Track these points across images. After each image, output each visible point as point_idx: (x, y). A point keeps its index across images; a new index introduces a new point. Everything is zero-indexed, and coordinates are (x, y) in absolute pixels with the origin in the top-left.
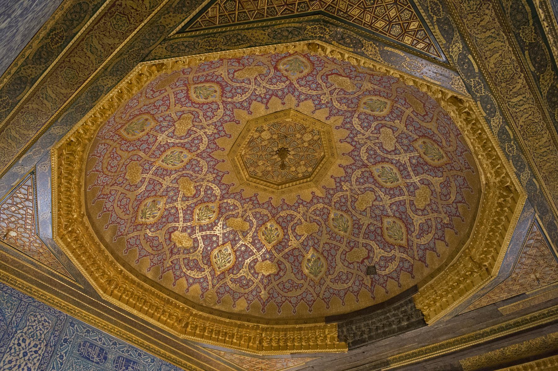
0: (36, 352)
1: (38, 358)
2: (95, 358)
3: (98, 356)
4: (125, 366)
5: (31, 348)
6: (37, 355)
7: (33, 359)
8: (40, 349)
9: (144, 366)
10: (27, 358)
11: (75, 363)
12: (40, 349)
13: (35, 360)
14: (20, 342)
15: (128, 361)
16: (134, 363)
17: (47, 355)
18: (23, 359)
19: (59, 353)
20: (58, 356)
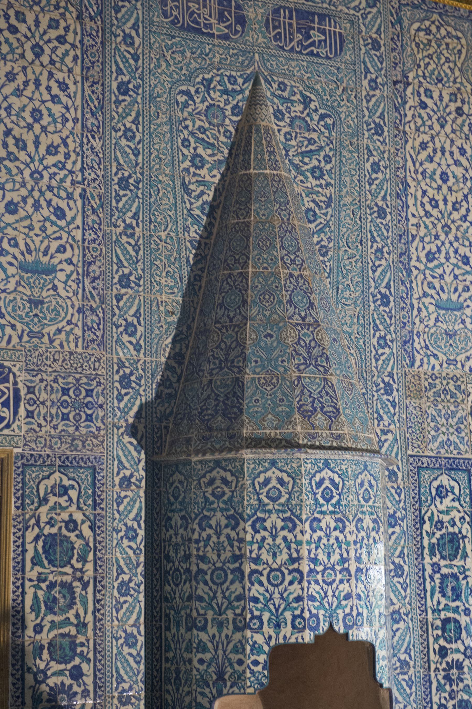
0: (61, 40)
1: (72, 53)
2: (215, 26)
3: (221, 18)
4: (299, 31)
5: (45, 33)
6: (68, 46)
7: (62, 60)
8: (67, 29)
9: (352, 22)
10: (45, 59)
11: (168, 48)
12: (67, 29)
13: (69, 60)
14: (13, 21)
16: (322, 17)
17: (92, 42)
18: (37, 62)
19: (119, 31)
20: (119, 39)
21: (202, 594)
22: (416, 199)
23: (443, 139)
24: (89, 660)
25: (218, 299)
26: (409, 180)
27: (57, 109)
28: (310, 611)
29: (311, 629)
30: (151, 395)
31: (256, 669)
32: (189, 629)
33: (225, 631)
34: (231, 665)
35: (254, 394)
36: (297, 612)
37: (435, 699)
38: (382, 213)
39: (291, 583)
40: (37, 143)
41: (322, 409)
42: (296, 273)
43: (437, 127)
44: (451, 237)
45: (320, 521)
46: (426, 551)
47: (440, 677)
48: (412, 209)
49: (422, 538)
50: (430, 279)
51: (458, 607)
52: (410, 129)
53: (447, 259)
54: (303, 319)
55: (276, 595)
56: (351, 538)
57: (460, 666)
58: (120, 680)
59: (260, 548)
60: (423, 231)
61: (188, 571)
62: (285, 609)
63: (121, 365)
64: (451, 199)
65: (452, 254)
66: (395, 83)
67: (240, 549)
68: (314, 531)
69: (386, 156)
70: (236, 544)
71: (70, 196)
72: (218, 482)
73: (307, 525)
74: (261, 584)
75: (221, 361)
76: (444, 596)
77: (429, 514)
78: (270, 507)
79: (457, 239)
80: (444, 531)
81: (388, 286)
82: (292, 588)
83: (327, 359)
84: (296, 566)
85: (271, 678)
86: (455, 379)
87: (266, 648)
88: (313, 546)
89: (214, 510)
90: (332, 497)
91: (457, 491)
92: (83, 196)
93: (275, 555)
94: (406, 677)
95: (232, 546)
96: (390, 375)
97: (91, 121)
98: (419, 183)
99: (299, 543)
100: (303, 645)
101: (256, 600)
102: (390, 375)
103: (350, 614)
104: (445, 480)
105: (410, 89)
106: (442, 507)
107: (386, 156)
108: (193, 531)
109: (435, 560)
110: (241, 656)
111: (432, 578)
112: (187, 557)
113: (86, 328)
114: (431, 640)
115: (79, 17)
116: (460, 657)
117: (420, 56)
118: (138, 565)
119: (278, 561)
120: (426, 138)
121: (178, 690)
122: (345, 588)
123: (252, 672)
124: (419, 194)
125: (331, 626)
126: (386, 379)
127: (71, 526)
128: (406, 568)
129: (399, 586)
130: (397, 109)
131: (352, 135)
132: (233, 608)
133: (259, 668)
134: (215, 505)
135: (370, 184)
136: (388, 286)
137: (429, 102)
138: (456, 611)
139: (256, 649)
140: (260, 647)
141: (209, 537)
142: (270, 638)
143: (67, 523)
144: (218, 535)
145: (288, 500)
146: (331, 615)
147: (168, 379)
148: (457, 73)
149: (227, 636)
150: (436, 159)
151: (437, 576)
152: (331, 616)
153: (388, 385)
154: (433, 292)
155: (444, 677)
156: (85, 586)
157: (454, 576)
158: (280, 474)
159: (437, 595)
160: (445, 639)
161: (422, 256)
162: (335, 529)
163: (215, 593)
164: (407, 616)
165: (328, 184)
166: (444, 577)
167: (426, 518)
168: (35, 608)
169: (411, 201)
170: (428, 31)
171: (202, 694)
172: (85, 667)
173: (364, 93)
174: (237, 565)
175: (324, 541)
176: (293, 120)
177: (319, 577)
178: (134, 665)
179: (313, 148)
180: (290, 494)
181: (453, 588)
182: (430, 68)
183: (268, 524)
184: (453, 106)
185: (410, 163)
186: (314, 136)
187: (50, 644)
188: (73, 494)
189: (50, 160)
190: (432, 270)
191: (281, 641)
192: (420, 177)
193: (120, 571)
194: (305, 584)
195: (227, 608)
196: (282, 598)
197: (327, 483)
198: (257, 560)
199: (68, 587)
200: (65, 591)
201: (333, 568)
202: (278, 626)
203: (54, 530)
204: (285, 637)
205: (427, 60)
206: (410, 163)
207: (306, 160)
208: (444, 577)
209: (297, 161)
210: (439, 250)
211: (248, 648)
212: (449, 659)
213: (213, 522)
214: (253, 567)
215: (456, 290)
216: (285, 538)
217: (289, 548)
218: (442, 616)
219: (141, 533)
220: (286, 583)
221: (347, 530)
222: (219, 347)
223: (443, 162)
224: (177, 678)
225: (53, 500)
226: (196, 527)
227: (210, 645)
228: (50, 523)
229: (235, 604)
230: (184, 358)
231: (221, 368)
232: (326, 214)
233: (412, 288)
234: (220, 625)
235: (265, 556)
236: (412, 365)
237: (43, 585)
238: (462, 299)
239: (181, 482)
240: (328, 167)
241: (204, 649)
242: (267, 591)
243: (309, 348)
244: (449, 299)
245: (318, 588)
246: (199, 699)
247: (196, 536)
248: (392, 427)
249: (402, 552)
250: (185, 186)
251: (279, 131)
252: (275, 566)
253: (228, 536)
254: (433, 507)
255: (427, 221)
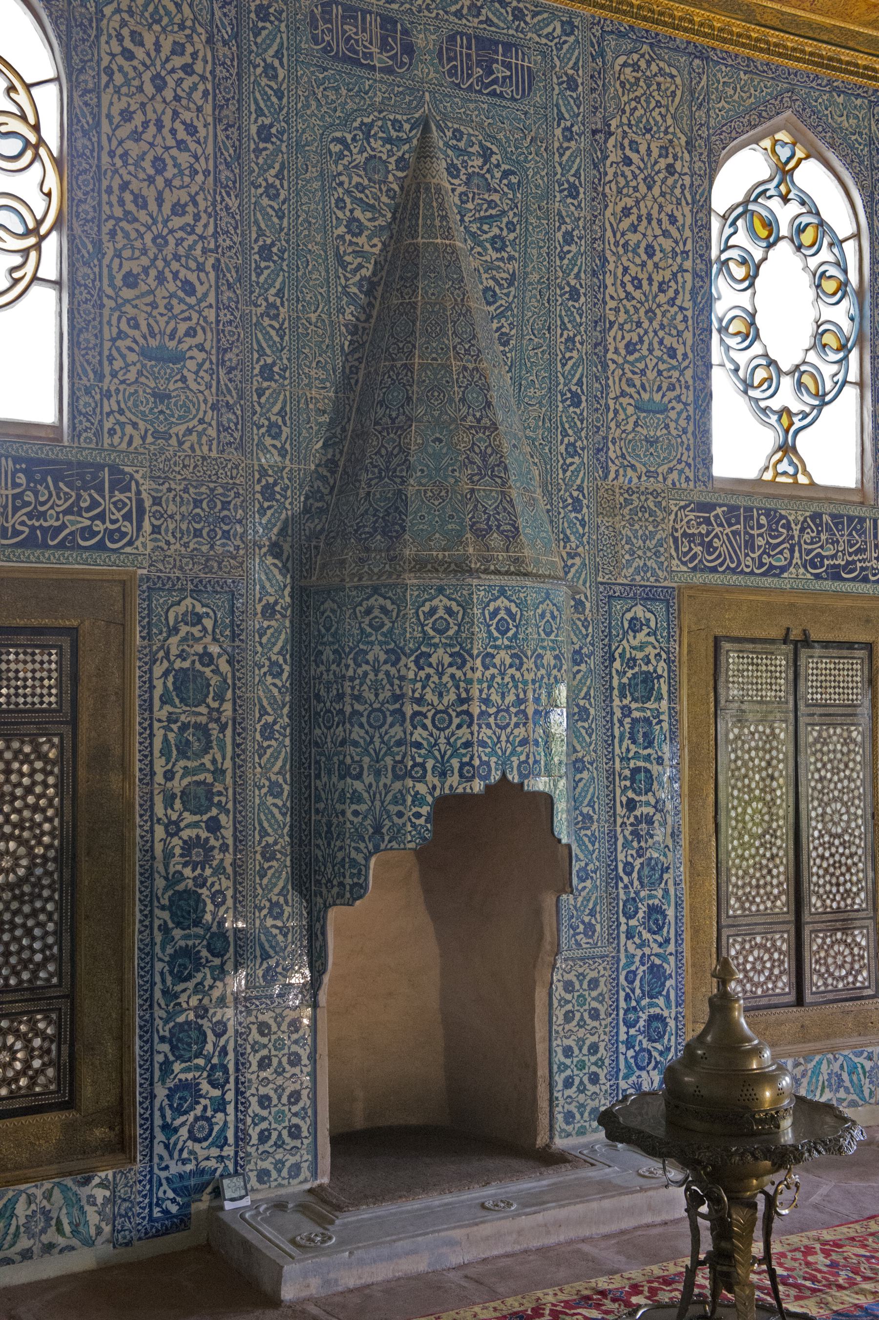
0: (188, 69)
1: (201, 87)
2: (376, 56)
3: (384, 46)
4: (479, 64)
5: (168, 60)
6: (195, 78)
7: (189, 94)
8: (194, 56)
9: (543, 54)
10: (168, 94)
11: (320, 83)
12: (194, 56)
13: (197, 96)
14: (128, 43)
15: (486, 44)
16: (508, 47)
17: (225, 74)
18: (158, 98)
19: (258, 60)
20: (259, 70)
21: (357, 738)
22: (615, 278)
23: (649, 204)
24: (227, 812)
25: (378, 395)
26: (608, 254)
27: (184, 158)
28: (480, 757)
29: (482, 778)
30: (298, 507)
31: (417, 822)
32: (342, 777)
33: (383, 780)
34: (389, 817)
35: (419, 509)
36: (466, 759)
37: (621, 857)
38: (574, 294)
39: (459, 727)
40: (160, 201)
41: (498, 527)
42: (471, 366)
43: (643, 188)
44: (656, 324)
45: (493, 657)
46: (616, 692)
47: (627, 833)
48: (610, 290)
49: (611, 678)
50: (629, 375)
51: (649, 755)
52: (610, 190)
53: (651, 351)
54: (479, 421)
55: (442, 740)
56: (529, 677)
57: (650, 821)
58: (264, 833)
59: (424, 687)
60: (622, 317)
61: (341, 712)
62: (451, 756)
63: (263, 473)
64: (656, 278)
65: (656, 346)
66: (594, 132)
67: (401, 688)
68: (486, 668)
69: (581, 223)
70: (396, 682)
71: (200, 268)
72: (376, 612)
73: (478, 662)
74: (425, 727)
75: (380, 470)
76: (634, 742)
77: (620, 650)
78: (437, 640)
79: (662, 327)
80: (637, 669)
81: (579, 383)
82: (460, 733)
83: (506, 468)
84: (465, 707)
85: (435, 832)
86: (655, 494)
87: (430, 799)
88: (485, 685)
89: (372, 643)
90: (508, 630)
91: (653, 624)
92: (216, 267)
93: (441, 695)
94: (589, 833)
95: (392, 685)
96: (580, 489)
97: (225, 173)
98: (619, 257)
99: (470, 682)
100: (473, 796)
101: (418, 745)
102: (580, 489)
103: (526, 762)
104: (639, 611)
105: (612, 141)
106: (635, 643)
107: (581, 223)
108: (347, 666)
109: (626, 702)
110: (401, 808)
111: (621, 722)
112: (340, 697)
113: (222, 428)
114: (618, 791)
115: (210, 41)
116: (651, 811)
117: (625, 98)
118: (284, 705)
119: (445, 701)
120: (630, 202)
121: (329, 844)
122: (520, 732)
123: (414, 826)
124: (620, 271)
125: (504, 775)
126: (575, 494)
127: (206, 660)
128: (592, 711)
129: (583, 732)
130: (595, 166)
131: (541, 198)
132: (393, 755)
133: (422, 821)
134: (373, 638)
135: (562, 259)
136: (579, 383)
137: (634, 157)
138: (647, 758)
139: (418, 800)
140: (423, 798)
141: (366, 674)
142: (434, 787)
143: (201, 657)
144: (376, 672)
145: (458, 632)
146: (505, 762)
147: (319, 491)
148: (670, 121)
149: (385, 785)
150: (641, 228)
151: (628, 720)
152: (504, 763)
153: (576, 500)
154: (632, 390)
155: (632, 833)
156: (223, 728)
157: (647, 720)
158: (448, 603)
159: (627, 742)
160: (634, 790)
161: (621, 346)
162: (511, 666)
163: (372, 738)
164: (591, 764)
165: (511, 258)
166: (635, 721)
167: (617, 655)
168: (166, 752)
169: (609, 281)
170: (636, 67)
171: (357, 849)
172: (223, 818)
173: (557, 145)
174: (397, 706)
175: (498, 679)
176: (470, 176)
177: (491, 720)
178: (279, 817)
179: (493, 212)
180: (459, 625)
181: (645, 735)
182: (637, 114)
183: (434, 660)
184: (663, 163)
185: (609, 233)
186: (495, 197)
187: (183, 792)
188: (208, 623)
189: (177, 222)
190: (632, 364)
191: (447, 791)
192: (621, 250)
193: (263, 712)
194: (475, 728)
195: (385, 754)
196: (449, 743)
197: (502, 614)
198: (420, 701)
199: (203, 729)
200: (200, 734)
201: (507, 710)
202: (443, 775)
203: (186, 664)
204: (451, 787)
205: (633, 104)
206: (609, 233)
207: (486, 227)
208: (635, 721)
209: (474, 228)
210: (641, 341)
211: (409, 799)
212: (638, 813)
213: (370, 657)
214: (416, 708)
215: (660, 388)
216: (453, 676)
217: (458, 687)
218: (632, 765)
219: (287, 668)
220: (454, 726)
221: (525, 667)
222: (378, 453)
223: (649, 232)
224: (329, 831)
225: (184, 629)
226: (350, 662)
227: (365, 795)
228: (182, 656)
229: (395, 749)
230: (337, 466)
231: (381, 478)
232: (507, 295)
233: (608, 385)
234: (378, 774)
235: (429, 696)
236: (606, 477)
237: (175, 727)
238: (666, 400)
239: (333, 611)
240: (512, 236)
241: (359, 800)
242: (431, 735)
243: (484, 456)
244: (651, 400)
245: (489, 732)
246: (353, 854)
247: (350, 673)
248: (580, 550)
249: (588, 693)
250: (339, 258)
251: (453, 190)
252: (441, 707)
253: (387, 673)
254: (624, 642)
255: (628, 305)
